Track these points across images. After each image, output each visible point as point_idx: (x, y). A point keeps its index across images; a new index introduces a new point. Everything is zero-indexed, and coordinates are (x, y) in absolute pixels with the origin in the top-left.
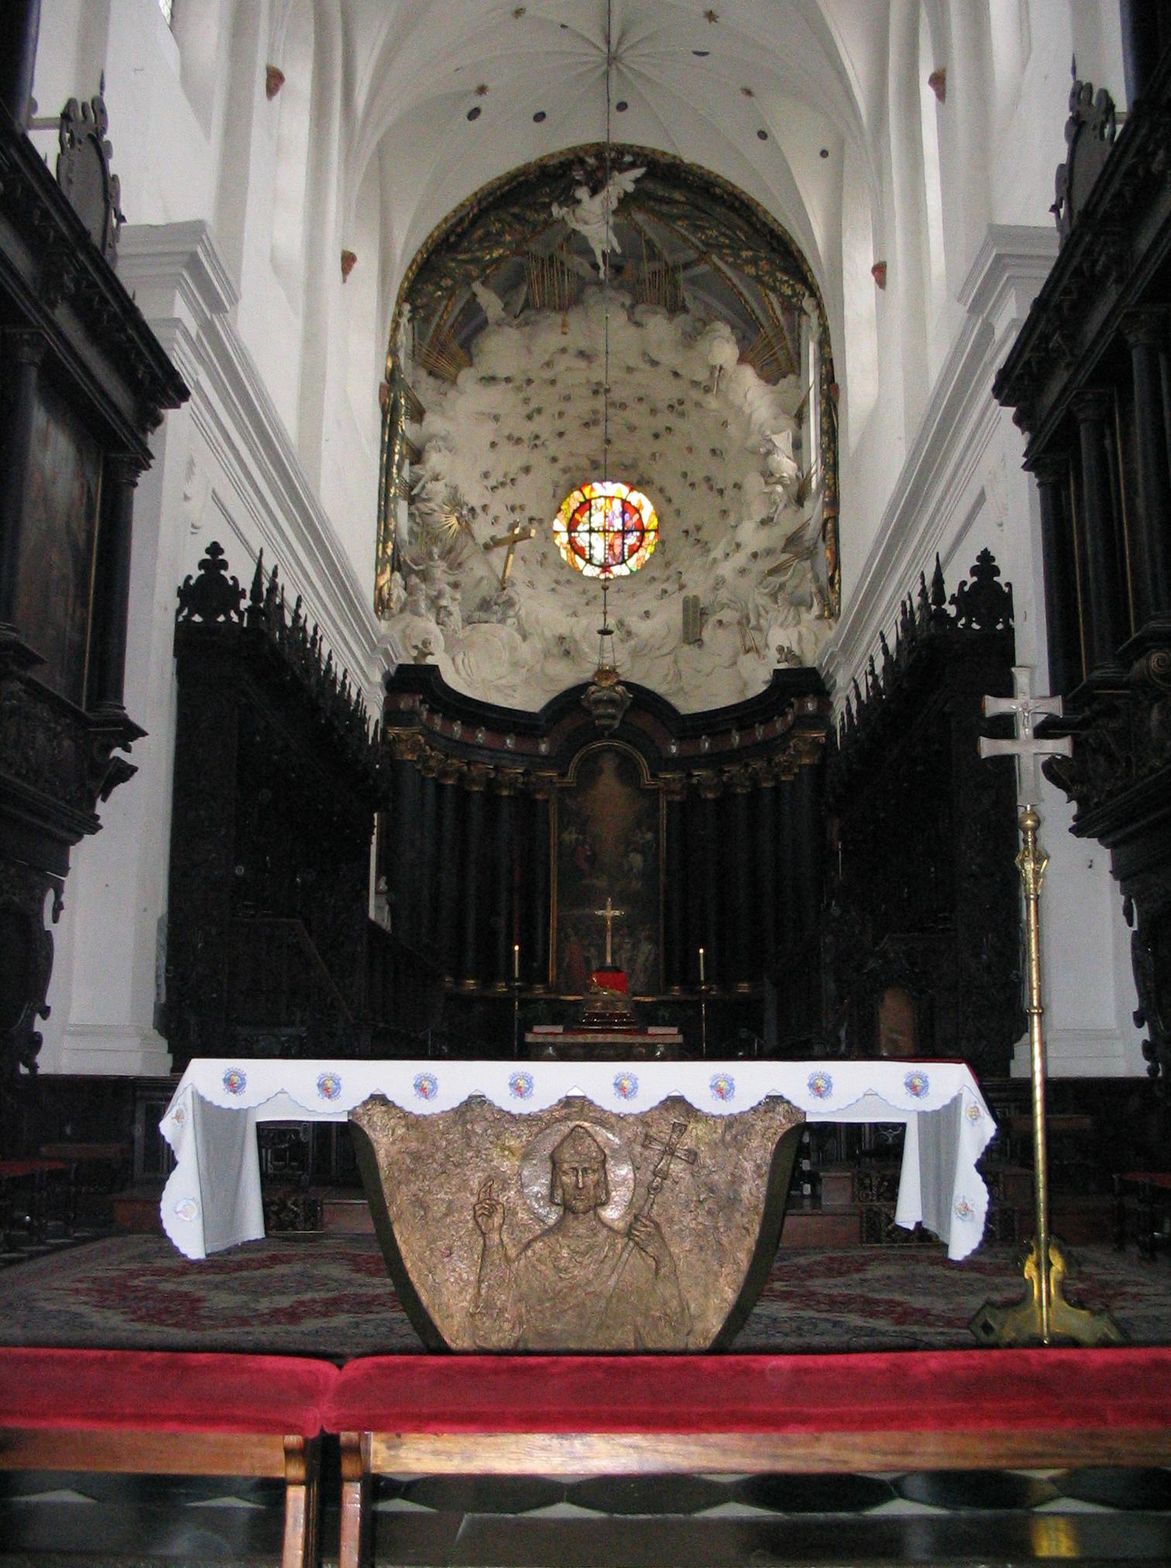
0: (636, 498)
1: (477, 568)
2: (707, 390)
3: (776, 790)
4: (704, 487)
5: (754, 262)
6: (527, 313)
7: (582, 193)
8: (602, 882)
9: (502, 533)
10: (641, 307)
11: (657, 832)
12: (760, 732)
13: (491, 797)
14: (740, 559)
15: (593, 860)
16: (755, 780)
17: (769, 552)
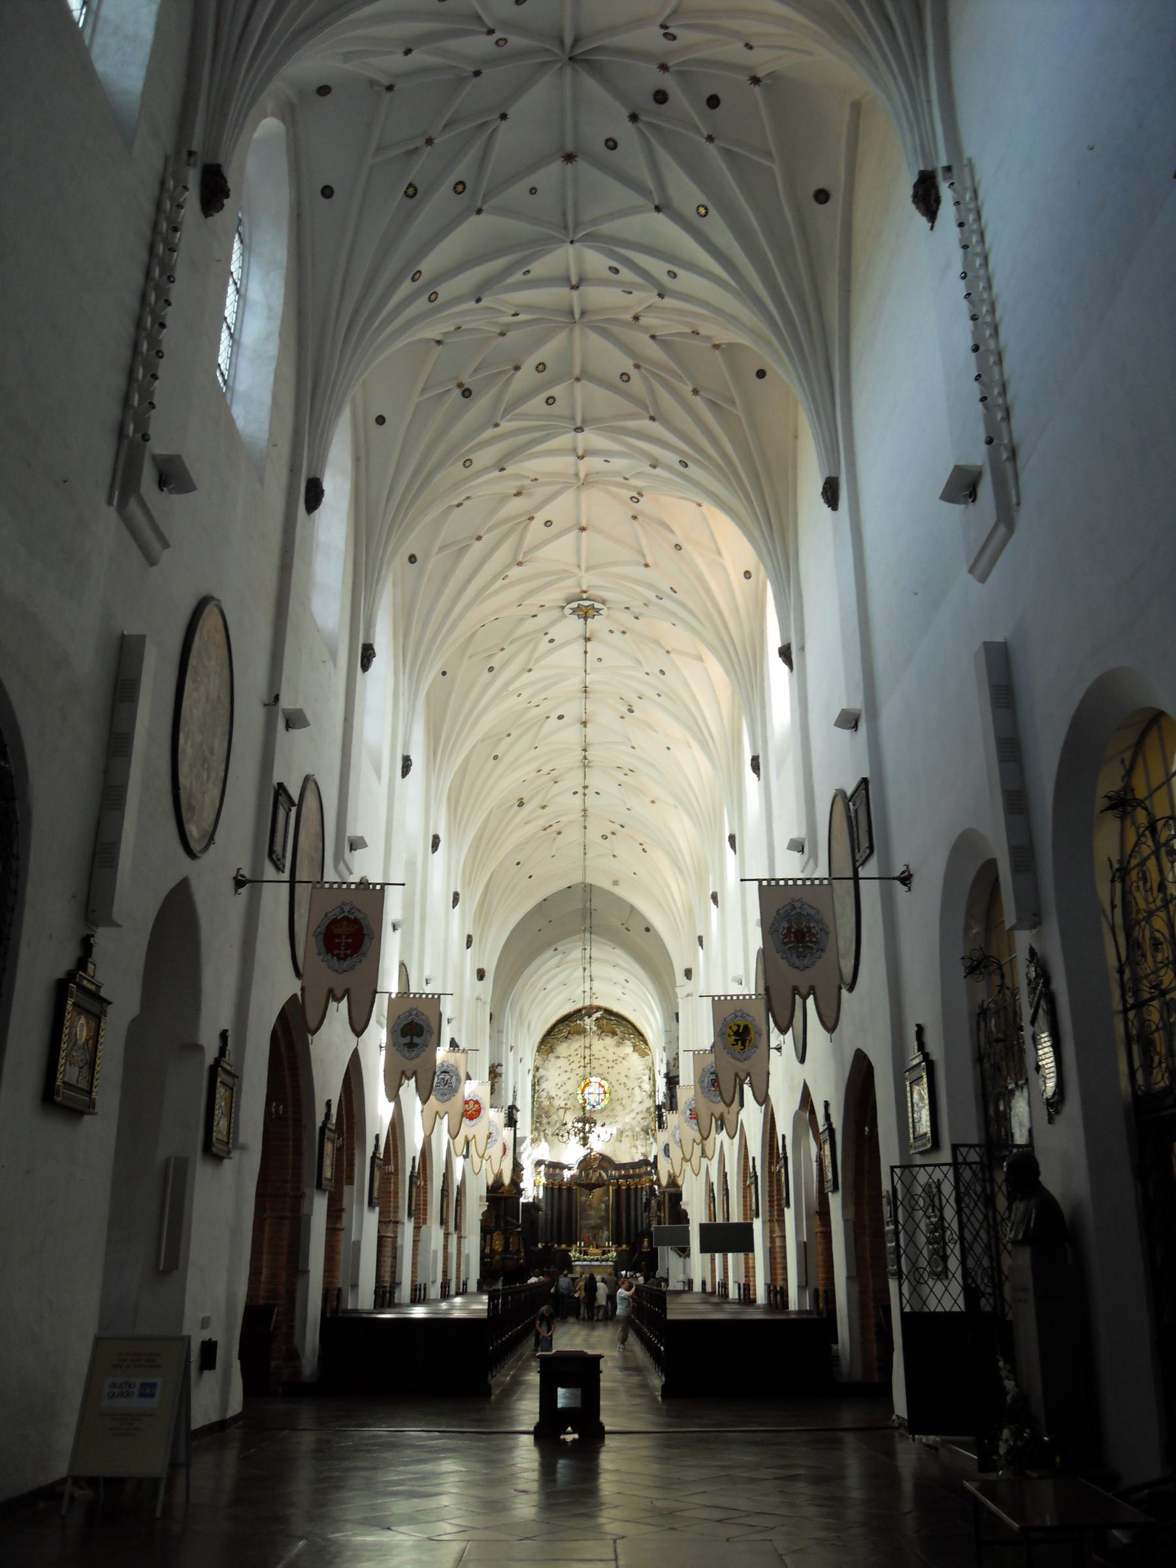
0: (603, 1083)
1: (554, 1118)
2: (624, 1058)
3: (642, 1188)
4: (623, 1086)
5: (634, 1038)
6: (569, 1035)
7: (586, 1018)
8: (592, 1213)
9: (562, 1105)
10: (603, 1034)
11: (609, 1196)
12: (637, 1170)
13: (560, 1189)
14: (633, 1114)
15: (590, 1206)
16: (636, 1184)
17: (642, 1112)
